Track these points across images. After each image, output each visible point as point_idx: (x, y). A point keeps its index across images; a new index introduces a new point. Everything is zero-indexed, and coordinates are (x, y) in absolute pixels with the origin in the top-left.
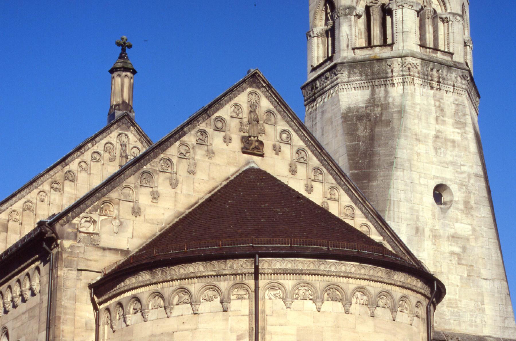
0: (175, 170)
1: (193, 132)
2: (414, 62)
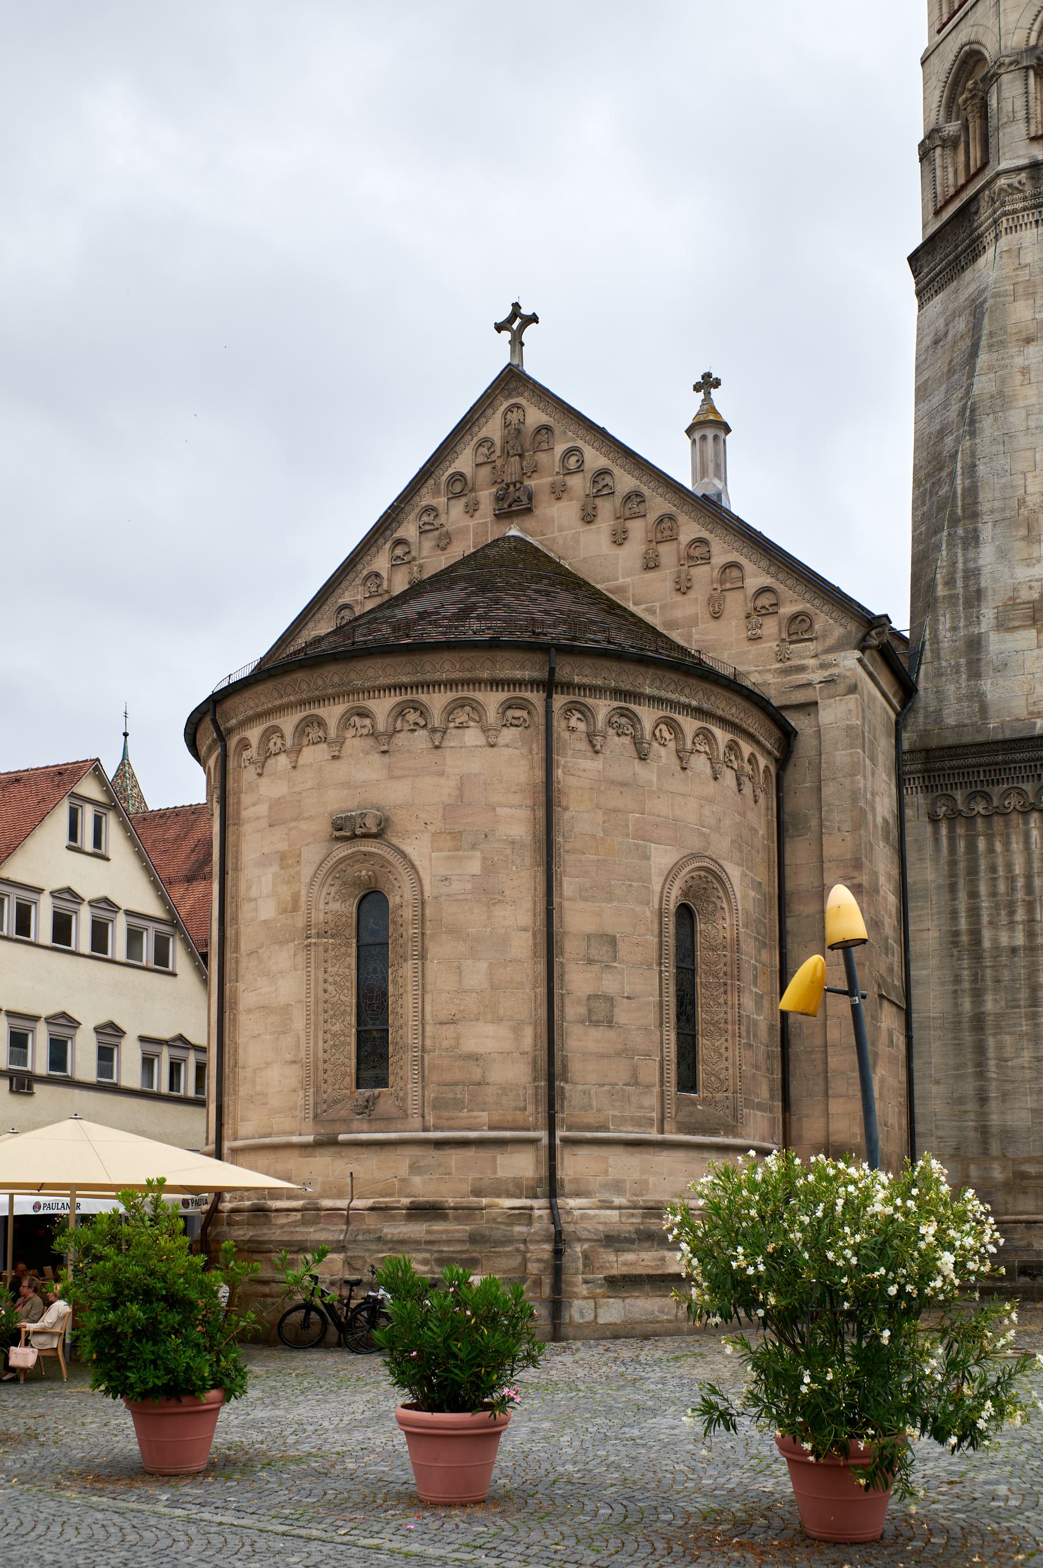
0: (385, 586)
1: (412, 516)
2: (1009, 181)
